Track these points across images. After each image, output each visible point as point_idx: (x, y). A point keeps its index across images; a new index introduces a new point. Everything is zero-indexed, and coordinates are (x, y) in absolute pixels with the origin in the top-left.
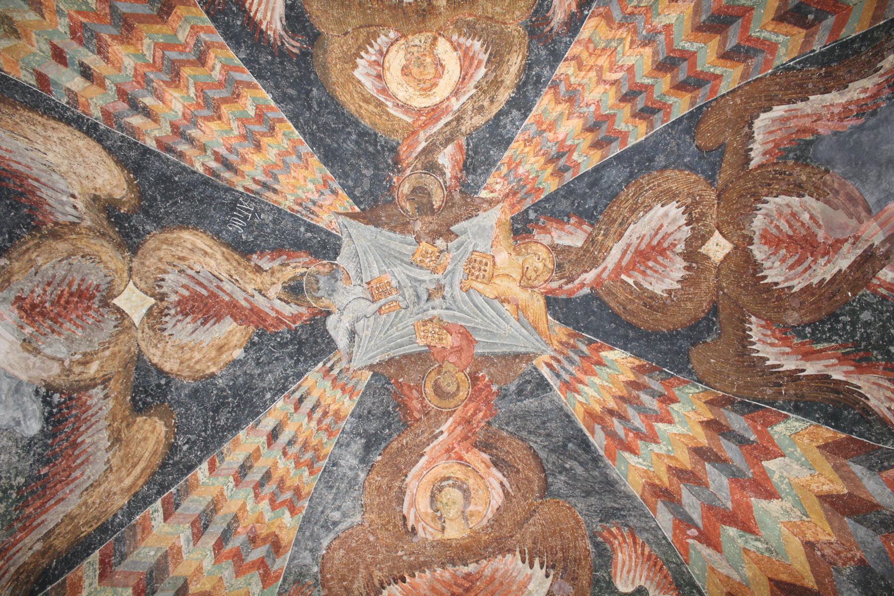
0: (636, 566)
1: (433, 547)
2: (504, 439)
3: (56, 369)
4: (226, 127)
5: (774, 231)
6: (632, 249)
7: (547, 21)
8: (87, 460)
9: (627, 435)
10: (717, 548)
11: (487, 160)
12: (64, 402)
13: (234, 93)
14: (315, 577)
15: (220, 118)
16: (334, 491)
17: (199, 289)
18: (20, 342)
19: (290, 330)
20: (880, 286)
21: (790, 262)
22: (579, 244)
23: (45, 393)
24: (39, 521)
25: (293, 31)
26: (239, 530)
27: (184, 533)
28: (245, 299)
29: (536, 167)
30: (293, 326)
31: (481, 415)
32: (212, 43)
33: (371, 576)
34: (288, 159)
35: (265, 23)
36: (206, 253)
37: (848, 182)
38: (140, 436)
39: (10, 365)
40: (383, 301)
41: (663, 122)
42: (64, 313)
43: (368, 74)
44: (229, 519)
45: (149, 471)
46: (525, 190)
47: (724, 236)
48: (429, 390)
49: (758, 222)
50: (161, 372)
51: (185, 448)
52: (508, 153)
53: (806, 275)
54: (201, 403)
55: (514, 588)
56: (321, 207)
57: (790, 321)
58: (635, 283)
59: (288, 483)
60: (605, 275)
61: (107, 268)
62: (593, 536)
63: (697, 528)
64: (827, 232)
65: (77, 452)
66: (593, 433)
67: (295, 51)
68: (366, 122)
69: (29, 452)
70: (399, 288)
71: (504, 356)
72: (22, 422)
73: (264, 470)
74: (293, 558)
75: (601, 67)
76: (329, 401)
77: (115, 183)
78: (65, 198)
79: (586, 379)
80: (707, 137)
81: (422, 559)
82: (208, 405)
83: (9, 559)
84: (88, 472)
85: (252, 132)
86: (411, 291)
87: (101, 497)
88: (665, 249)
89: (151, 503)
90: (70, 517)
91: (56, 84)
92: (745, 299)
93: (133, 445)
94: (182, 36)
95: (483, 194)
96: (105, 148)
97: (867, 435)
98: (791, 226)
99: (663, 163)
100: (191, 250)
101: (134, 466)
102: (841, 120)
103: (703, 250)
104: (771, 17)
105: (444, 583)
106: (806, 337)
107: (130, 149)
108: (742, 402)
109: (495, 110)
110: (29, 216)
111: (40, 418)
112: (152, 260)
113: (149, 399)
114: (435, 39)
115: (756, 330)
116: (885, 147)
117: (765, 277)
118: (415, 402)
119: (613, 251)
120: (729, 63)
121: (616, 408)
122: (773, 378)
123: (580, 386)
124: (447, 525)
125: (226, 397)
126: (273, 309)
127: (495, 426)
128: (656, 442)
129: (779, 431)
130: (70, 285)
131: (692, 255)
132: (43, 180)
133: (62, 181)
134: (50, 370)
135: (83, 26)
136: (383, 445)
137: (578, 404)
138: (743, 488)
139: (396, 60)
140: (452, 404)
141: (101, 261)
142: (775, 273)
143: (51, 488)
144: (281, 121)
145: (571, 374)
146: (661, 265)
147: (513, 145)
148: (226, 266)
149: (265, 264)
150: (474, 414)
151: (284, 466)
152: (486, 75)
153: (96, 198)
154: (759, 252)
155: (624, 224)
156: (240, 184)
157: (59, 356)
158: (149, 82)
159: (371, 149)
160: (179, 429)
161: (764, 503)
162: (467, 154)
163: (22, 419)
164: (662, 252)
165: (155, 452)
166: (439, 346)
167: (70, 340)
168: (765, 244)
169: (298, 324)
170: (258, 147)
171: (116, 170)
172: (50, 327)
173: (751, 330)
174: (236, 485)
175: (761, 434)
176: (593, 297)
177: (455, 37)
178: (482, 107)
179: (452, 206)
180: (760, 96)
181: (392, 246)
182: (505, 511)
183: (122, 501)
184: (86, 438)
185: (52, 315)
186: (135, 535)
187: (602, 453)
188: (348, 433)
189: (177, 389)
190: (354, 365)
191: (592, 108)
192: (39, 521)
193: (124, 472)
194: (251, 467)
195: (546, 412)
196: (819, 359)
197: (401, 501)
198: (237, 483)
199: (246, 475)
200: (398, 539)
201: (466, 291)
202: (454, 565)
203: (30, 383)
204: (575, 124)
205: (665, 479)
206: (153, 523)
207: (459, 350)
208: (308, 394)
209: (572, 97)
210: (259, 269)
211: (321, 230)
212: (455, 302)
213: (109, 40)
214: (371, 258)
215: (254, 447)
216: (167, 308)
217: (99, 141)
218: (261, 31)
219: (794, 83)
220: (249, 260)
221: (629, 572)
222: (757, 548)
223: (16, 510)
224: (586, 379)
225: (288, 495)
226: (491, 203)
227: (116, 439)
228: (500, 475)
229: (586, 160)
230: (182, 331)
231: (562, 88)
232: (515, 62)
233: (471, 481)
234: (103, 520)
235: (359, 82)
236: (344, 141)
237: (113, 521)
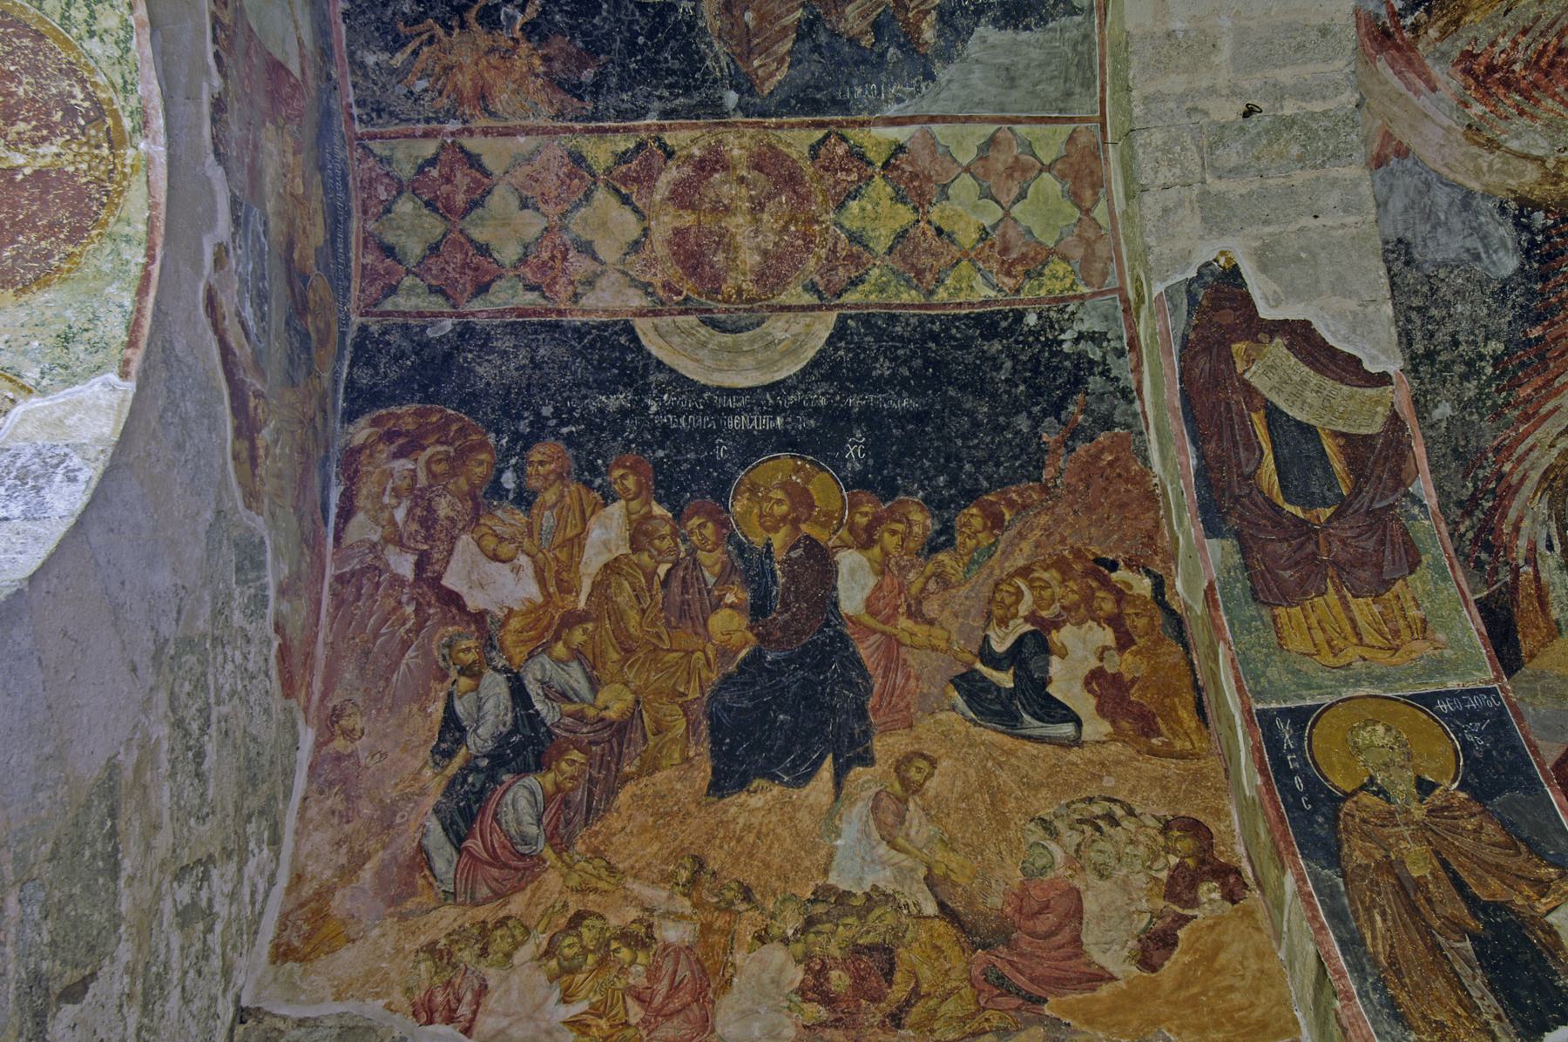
3: (1532, 173)
12: (1555, 225)
18: (1461, 130)
23: (1521, 210)
24: (1549, 406)
39: (1446, 165)
42: (1544, 82)
69: (1503, 302)
72: (1483, 255)
111: (1515, 250)
134: (1521, 174)
143: (1556, 358)
157: (1535, 152)
163: (1481, 250)
172: (1517, 106)
185: (1523, 84)
192: (1549, 406)
203: (1487, 196)
223: (1499, 391)
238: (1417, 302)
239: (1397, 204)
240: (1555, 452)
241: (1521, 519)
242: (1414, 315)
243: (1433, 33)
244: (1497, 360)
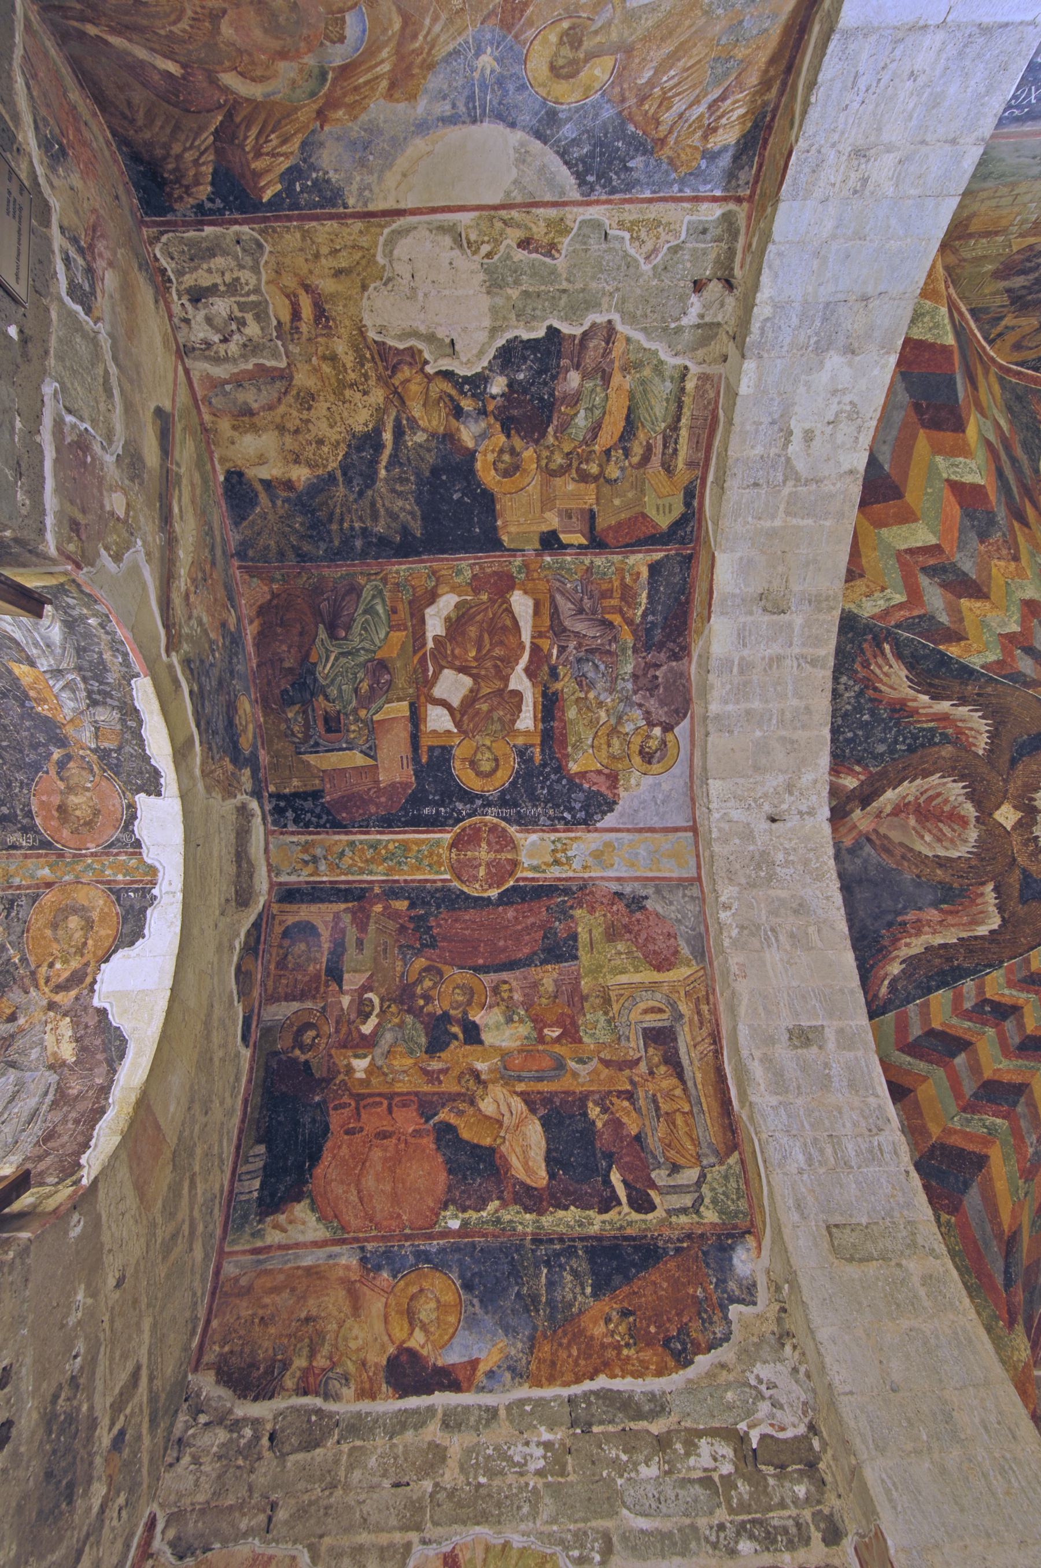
21: (939, 800)
49: (973, 834)
57: (950, 748)
103: (1020, 814)
115: (981, 744)
122: (981, 700)
129: (992, 657)
142: (955, 790)
154: (969, 810)
219: (977, 956)
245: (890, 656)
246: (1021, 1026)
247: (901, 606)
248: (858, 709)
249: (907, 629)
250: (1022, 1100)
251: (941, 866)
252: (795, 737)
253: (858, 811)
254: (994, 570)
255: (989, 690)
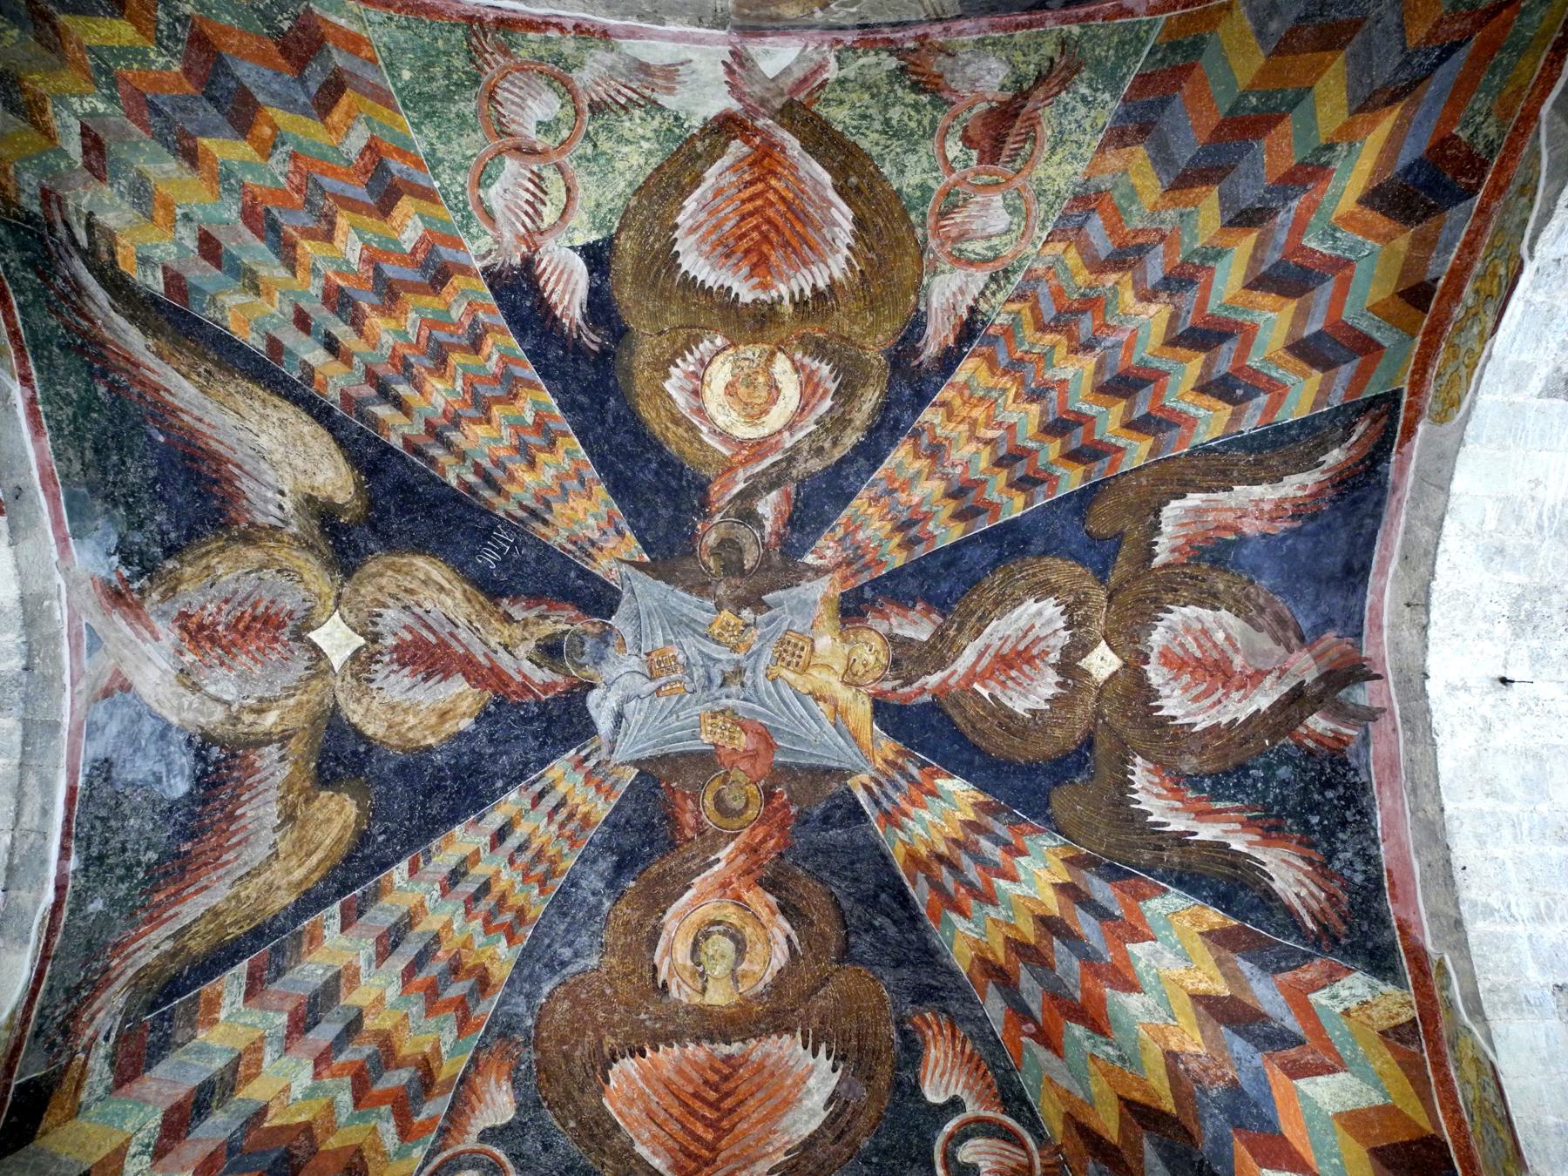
0: (953, 1067)
1: (688, 1013)
2: (798, 878)
3: (219, 713)
4: (495, 434)
5: (1178, 650)
6: (992, 651)
7: (917, 353)
8: (246, 839)
9: (957, 891)
10: (1057, 1050)
11: (819, 515)
12: (225, 759)
13: (510, 392)
14: (527, 1032)
15: (489, 421)
16: (568, 919)
17: (425, 633)
19: (538, 702)
20: (1307, 736)
22: (925, 638)
23: (200, 745)
24: (171, 912)
25: (595, 323)
26: (439, 954)
27: (368, 948)
28: (485, 655)
29: (881, 534)
30: (544, 698)
31: (772, 842)
32: (492, 325)
33: (600, 1042)
34: (567, 484)
35: (560, 308)
36: (442, 589)
37: (1278, 598)
38: (321, 817)
40: (663, 680)
41: (1046, 497)
43: (682, 388)
44: (427, 939)
45: (328, 863)
46: (862, 561)
47: (1113, 649)
48: (708, 801)
49: (1158, 638)
50: (360, 735)
51: (381, 838)
52: (846, 512)
53: (1214, 711)
54: (409, 782)
55: (789, 1082)
56: (601, 549)
57: (1185, 768)
58: (991, 695)
59: (511, 901)
60: (952, 682)
61: (309, 590)
62: (899, 1023)
63: (1035, 1022)
64: (1245, 658)
65: (233, 828)
66: (914, 883)
67: (595, 348)
68: (672, 449)
69: (168, 819)
70: (688, 666)
71: (811, 769)
73: (482, 880)
74: (502, 1003)
75: (976, 420)
76: (578, 800)
77: (340, 484)
78: (270, 494)
79: (913, 811)
80: (1101, 521)
81: (671, 1028)
82: (418, 786)
83: (127, 957)
84: (245, 857)
85: (526, 444)
86: (701, 671)
87: (259, 890)
88: (1034, 657)
89: (326, 906)
90: (214, 913)
91: (290, 353)
92: (1132, 734)
93: (310, 828)
94: (456, 313)
95: (809, 559)
96: (336, 439)
97: (1265, 925)
98: (1200, 646)
99: (1041, 549)
100: (424, 582)
101: (309, 855)
102: (1272, 520)
103: (1083, 664)
104: (1191, 386)
105: (694, 1064)
106: (1203, 791)
107: (368, 444)
108: (1110, 866)
109: (837, 454)
110: (218, 510)
112: (370, 588)
113: (340, 769)
114: (773, 354)
115: (1141, 774)
116: (1326, 560)
117: (1160, 708)
118: (688, 816)
119: (967, 652)
120: (1135, 434)
121: (947, 852)
123: (905, 820)
124: (710, 985)
125: (443, 779)
126: (520, 672)
127: (789, 860)
128: (995, 905)
129: (1155, 907)
130: (255, 606)
131: (1068, 667)
132: (247, 468)
133: (271, 472)
134: (211, 714)
135: (340, 290)
136: (640, 867)
137: (898, 843)
138: (1097, 974)
139: (720, 373)
140: (737, 825)
141: (302, 580)
142: (1175, 703)
144: (565, 434)
145: (895, 803)
146: (1027, 676)
147: (855, 502)
148: (466, 608)
149: (517, 612)
150: (764, 841)
151: (508, 877)
152: (832, 408)
153: (310, 499)
154: (1155, 674)
155: (984, 620)
156: (501, 507)
157: (226, 697)
158: (407, 366)
159: (674, 483)
160: (374, 814)
161: (1122, 997)
162: (795, 506)
164: (1030, 660)
165: (339, 840)
166: (729, 747)
167: (244, 677)
168: (1164, 664)
169: (550, 695)
170: (532, 464)
171: (344, 468)
172: (219, 658)
173: (1133, 773)
174: (443, 896)
175: (1130, 910)
176: (934, 707)
177: (798, 356)
178: (822, 448)
179: (767, 570)
180: (1175, 478)
181: (685, 611)
182: (790, 973)
183: (285, 899)
184: (248, 811)
186: (300, 945)
187: (923, 910)
188: (596, 846)
189: (379, 760)
190: (617, 757)
191: (959, 470)
192: (171, 912)
193: (294, 862)
194: (465, 874)
195: (857, 849)
196: (1215, 821)
197: (653, 943)
198: (445, 892)
199: (456, 883)
200: (642, 996)
201: (773, 680)
202: (712, 1042)
203: (180, 730)
204: (935, 487)
205: (1000, 954)
206: (326, 932)
207: (753, 756)
208: (552, 787)
209: (936, 452)
210: (508, 619)
211: (596, 578)
212: (756, 691)
213: (368, 310)
214: (656, 623)
215: (472, 848)
216: (380, 653)
217: (331, 430)
218: (555, 318)
219: (1218, 466)
220: (497, 605)
221: (942, 1075)
222: (1107, 1054)
223: (141, 894)
224: (913, 811)
225: (508, 917)
226: (819, 572)
227: (289, 817)
228: (787, 926)
229: (946, 533)
230: (395, 685)
231: (925, 440)
232: (870, 398)
233: (748, 931)
234: (258, 921)
235: (670, 396)
236: (642, 469)
237: (272, 923)
238: (103, 813)
239: (113, 728)
240: (156, 953)
241: (99, 1010)
242: (98, 824)
243: (155, 596)
244: (149, 866)
245: (1303, 912)
246: (1207, 366)
247: (1314, 987)
248: (1329, 833)
249: (1292, 952)
250: (1264, 268)
251: (1215, 596)
252: (1491, 801)
253: (1308, 680)
254: (1198, 1038)
255: (1147, 856)
